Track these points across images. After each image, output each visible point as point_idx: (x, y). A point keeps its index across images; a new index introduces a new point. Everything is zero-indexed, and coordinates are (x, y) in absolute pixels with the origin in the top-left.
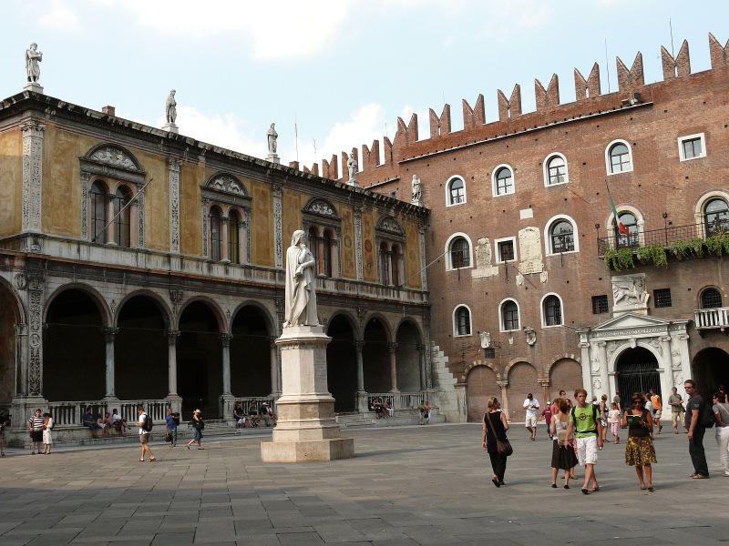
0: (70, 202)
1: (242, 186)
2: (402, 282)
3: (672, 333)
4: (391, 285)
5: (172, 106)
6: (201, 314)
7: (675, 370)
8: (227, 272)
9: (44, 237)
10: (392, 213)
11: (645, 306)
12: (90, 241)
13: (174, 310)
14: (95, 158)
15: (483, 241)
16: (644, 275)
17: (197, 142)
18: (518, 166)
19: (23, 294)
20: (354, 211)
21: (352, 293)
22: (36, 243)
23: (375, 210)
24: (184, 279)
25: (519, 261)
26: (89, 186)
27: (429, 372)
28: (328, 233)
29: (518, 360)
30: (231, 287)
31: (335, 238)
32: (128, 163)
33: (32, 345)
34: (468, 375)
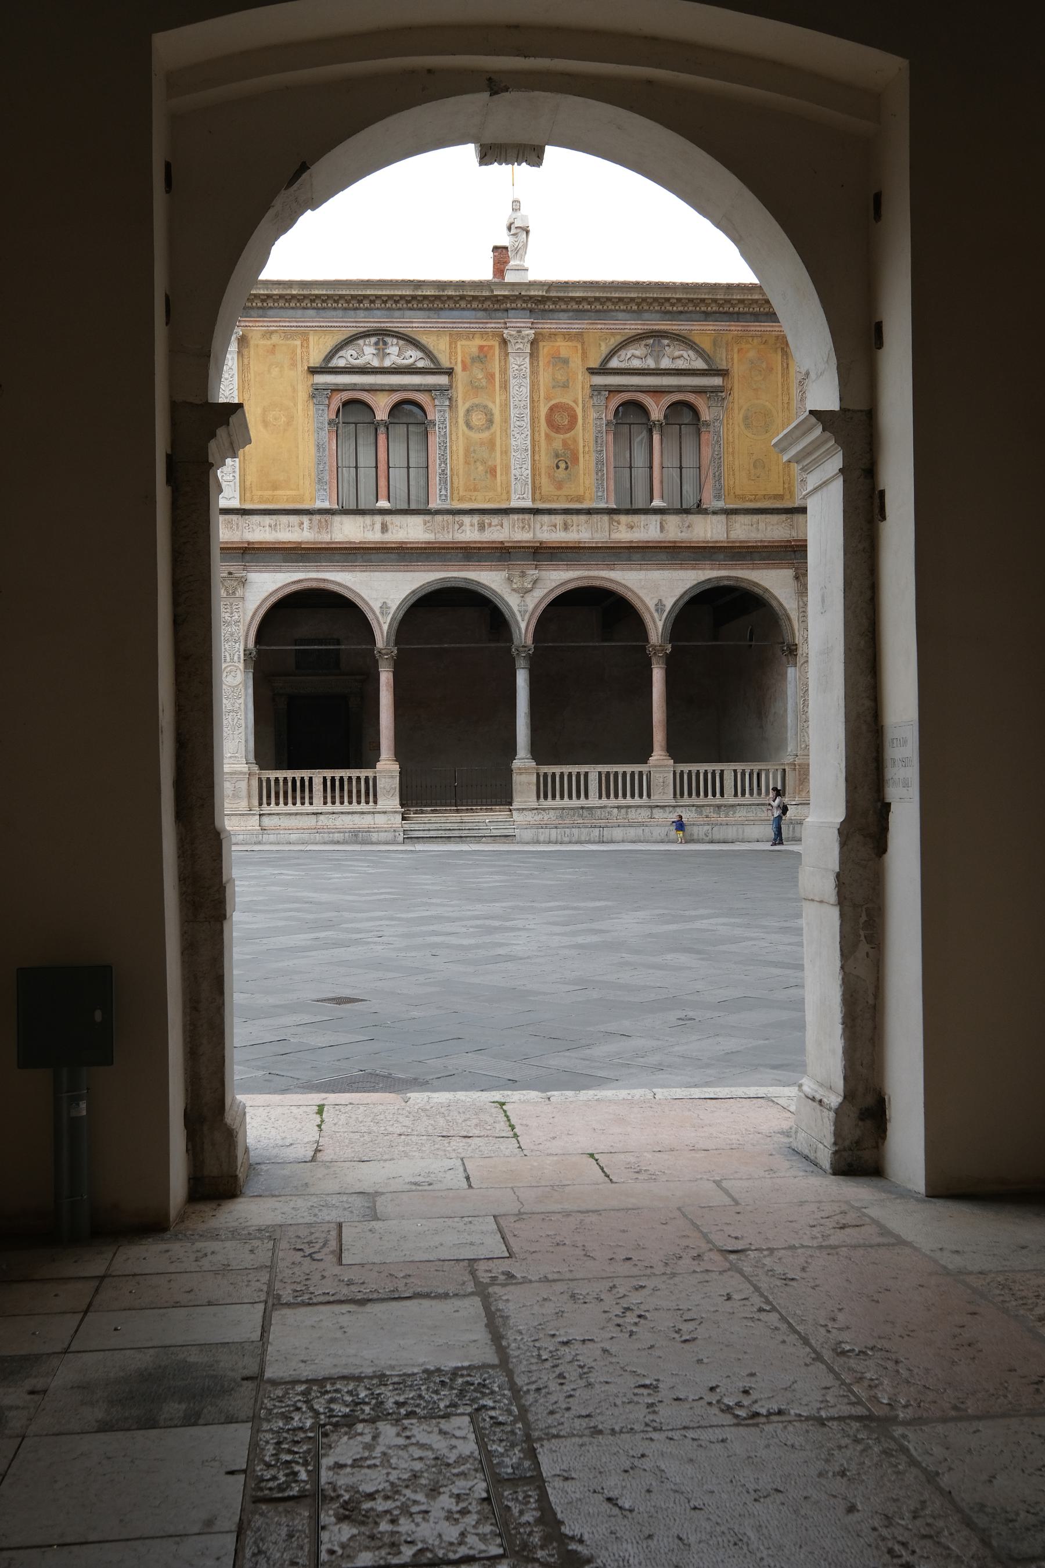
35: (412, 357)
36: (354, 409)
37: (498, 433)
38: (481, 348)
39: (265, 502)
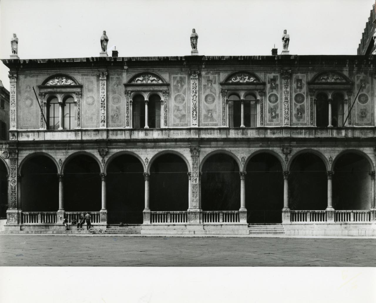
1: (159, 78)
8: (146, 134)
9: (18, 132)
14: (48, 85)
21: (274, 136)
24: (109, 143)
30: (149, 144)
32: (70, 82)
33: (12, 185)
35: (252, 79)
37: (279, 103)
38: (274, 76)
39: (206, 125)
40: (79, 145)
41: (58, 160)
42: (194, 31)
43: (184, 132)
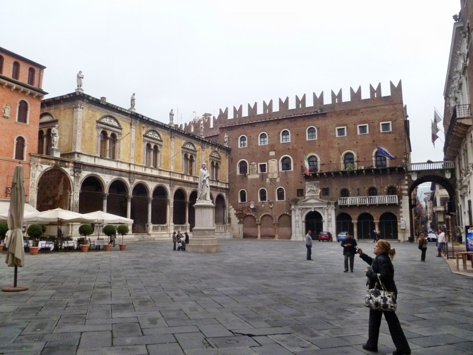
0: (92, 139)
1: (159, 136)
2: (219, 178)
3: (329, 206)
4: (215, 179)
5: (133, 100)
6: (141, 189)
7: (330, 221)
8: (152, 171)
10: (216, 149)
11: (319, 194)
12: (99, 156)
13: (131, 187)
15: (253, 163)
16: (318, 182)
17: (143, 116)
18: (270, 134)
19: (72, 178)
20: (202, 148)
22: (78, 156)
23: (210, 148)
25: (268, 173)
26: (100, 132)
27: (227, 216)
28: (191, 157)
29: (265, 213)
31: (194, 159)
32: (116, 124)
34: (244, 219)
35: (193, 148)
36: (186, 156)
40: (118, 172)
41: (105, 182)
42: (172, 110)
43: (168, 173)
